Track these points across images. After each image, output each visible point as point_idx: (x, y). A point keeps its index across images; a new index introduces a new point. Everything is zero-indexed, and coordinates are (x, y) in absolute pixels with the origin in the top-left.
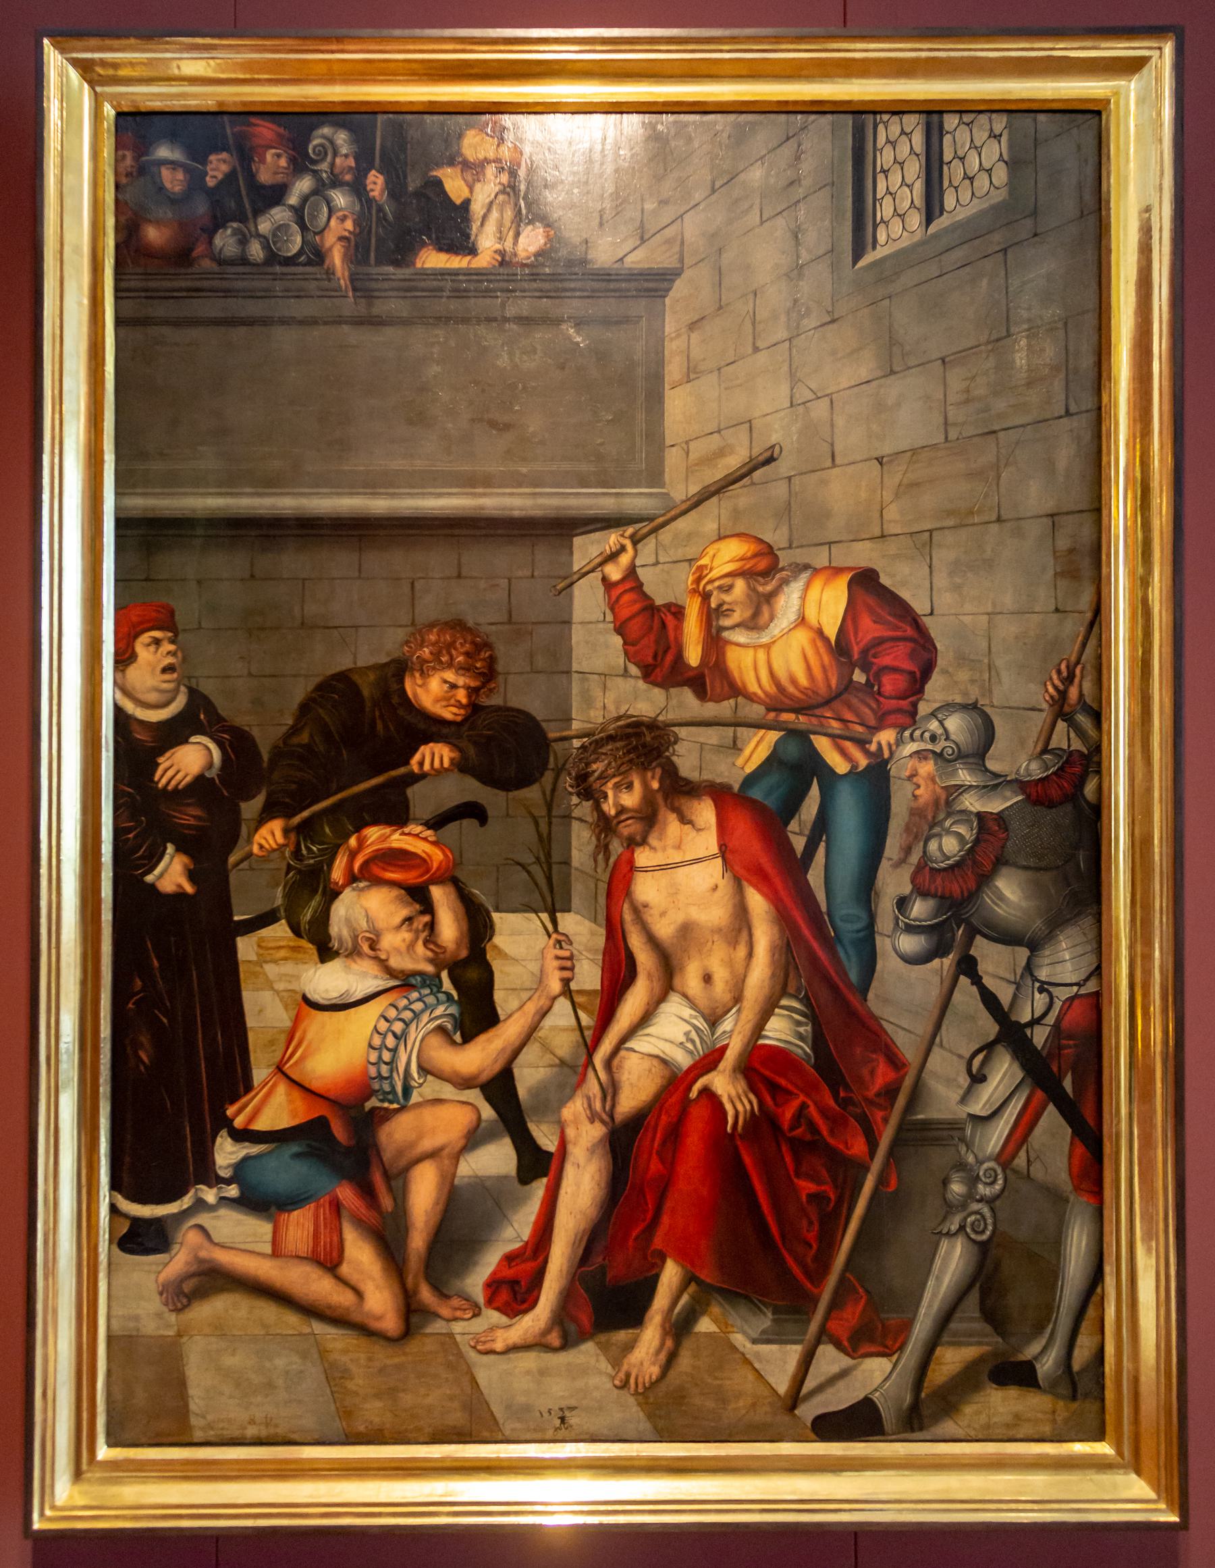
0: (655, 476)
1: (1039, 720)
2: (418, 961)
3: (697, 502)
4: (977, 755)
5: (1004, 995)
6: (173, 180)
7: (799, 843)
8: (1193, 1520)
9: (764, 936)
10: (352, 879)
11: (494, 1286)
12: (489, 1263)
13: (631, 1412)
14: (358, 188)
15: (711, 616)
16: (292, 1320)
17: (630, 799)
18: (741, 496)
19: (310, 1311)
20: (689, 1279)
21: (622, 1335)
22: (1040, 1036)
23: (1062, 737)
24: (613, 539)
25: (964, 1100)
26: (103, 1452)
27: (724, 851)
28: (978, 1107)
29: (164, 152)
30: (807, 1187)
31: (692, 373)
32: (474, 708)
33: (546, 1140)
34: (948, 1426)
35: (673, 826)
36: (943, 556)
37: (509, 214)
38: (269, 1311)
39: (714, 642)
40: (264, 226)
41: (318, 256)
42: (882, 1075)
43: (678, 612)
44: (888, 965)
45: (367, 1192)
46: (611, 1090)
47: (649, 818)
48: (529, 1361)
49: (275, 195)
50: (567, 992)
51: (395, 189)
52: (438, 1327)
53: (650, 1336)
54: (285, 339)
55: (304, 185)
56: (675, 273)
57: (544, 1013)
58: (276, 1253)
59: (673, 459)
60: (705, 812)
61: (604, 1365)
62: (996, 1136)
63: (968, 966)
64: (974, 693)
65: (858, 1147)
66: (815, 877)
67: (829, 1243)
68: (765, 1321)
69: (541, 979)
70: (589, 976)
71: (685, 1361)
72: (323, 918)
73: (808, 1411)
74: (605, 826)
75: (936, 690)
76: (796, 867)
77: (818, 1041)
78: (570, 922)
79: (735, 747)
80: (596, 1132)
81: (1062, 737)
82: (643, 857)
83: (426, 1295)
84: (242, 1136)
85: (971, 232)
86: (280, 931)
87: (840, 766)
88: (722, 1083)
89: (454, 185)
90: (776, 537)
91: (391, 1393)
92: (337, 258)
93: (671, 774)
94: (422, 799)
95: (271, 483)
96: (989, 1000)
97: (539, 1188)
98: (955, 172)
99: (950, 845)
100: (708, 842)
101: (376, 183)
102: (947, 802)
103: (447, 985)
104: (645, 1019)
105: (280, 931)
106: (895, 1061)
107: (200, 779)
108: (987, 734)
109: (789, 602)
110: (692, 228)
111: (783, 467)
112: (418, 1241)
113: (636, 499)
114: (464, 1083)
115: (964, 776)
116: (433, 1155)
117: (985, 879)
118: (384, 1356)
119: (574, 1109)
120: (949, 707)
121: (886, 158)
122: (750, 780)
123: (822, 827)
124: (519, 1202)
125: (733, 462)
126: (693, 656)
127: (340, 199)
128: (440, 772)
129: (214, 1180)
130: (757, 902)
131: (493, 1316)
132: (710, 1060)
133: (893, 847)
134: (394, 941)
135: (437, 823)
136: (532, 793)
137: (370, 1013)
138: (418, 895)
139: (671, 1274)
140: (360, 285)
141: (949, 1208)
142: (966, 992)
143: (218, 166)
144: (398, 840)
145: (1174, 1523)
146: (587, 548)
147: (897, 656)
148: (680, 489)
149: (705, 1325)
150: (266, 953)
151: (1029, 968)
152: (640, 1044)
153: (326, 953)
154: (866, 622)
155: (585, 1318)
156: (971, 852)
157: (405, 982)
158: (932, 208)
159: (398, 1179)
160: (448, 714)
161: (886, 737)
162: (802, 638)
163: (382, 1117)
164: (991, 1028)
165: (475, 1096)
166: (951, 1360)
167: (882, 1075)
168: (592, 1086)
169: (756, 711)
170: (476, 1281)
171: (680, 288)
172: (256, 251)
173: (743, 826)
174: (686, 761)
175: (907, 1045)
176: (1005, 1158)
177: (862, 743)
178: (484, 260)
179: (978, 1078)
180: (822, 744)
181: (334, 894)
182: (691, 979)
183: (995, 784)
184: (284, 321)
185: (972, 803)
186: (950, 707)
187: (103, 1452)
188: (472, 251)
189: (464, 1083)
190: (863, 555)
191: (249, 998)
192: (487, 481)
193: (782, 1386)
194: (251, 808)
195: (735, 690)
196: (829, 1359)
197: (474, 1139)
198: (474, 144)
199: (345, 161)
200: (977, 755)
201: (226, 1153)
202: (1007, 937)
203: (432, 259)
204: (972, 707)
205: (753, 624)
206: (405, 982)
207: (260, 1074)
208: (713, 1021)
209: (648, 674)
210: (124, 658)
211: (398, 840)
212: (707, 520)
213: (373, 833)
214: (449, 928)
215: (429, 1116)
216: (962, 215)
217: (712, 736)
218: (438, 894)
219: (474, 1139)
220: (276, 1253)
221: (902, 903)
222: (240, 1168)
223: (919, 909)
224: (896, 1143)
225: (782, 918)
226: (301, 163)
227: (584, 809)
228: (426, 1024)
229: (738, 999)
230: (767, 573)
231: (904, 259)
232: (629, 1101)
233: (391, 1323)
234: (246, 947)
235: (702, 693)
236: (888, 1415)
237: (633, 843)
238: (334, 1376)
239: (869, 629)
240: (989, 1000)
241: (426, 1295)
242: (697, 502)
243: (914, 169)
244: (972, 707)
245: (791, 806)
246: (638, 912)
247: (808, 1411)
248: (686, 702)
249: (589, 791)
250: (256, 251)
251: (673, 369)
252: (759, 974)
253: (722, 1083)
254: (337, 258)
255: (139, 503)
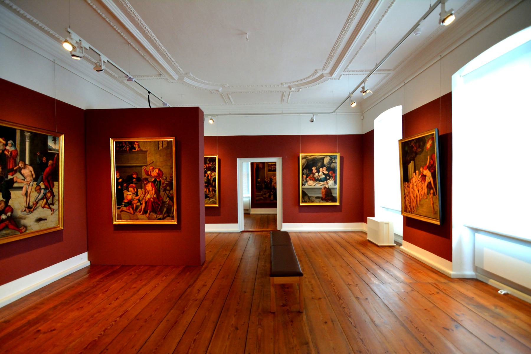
0: (147, 163)
1: (170, 177)
2: (134, 192)
3: (149, 164)
4: (166, 180)
5: (168, 194)
6: (118, 146)
7: (156, 185)
8: (183, 223)
9: (154, 191)
10: (130, 187)
11: (139, 211)
12: (138, 210)
13: (147, 219)
14: (129, 146)
15: (150, 171)
16: (127, 213)
17: (146, 182)
18: (152, 164)
19: (128, 213)
20: (150, 211)
21: (146, 214)
22: (170, 196)
23: (171, 178)
24: (144, 167)
25: (166, 200)
26: (117, 220)
27: (151, 185)
28: (167, 200)
29: (118, 144)
30: (157, 205)
31: (149, 157)
32: (136, 177)
33: (141, 203)
34: (165, 219)
35: (148, 184)
36: (164, 168)
37: (138, 147)
38: (126, 212)
39: (150, 173)
40: (124, 148)
41: (126, 150)
42: (161, 199)
43: (148, 171)
44: (161, 192)
45: (131, 206)
46: (145, 200)
47: (147, 184)
48: (141, 216)
49: (124, 146)
50: (142, 194)
51: (131, 146)
52: (135, 214)
53: (148, 214)
54: (125, 155)
55: (126, 146)
56: (147, 151)
57: (141, 195)
58: (126, 209)
59: (148, 162)
60: (150, 183)
61: (145, 216)
62: (167, 202)
63: (166, 192)
64: (166, 176)
65: (159, 203)
66: (157, 187)
67: (158, 208)
68: (154, 213)
69: (141, 193)
70: (144, 193)
71: (150, 215)
72: (128, 190)
73: (157, 218)
74: (144, 184)
75: (164, 176)
76: (156, 186)
77: (157, 197)
78: (142, 190)
79: (152, 179)
80: (144, 202)
81: (171, 178)
82: (147, 186)
83: (135, 212)
84: (124, 202)
85: (165, 148)
86: (126, 190)
87: (158, 180)
88: (152, 199)
89: (135, 146)
90: (154, 167)
91: (133, 217)
92: (128, 150)
93: (148, 181)
94: (134, 183)
95: (125, 164)
96: (167, 194)
97: (141, 205)
98: (164, 145)
99: (164, 185)
100: (151, 185)
101: (130, 146)
102: (164, 183)
103: (135, 193)
104: (147, 196)
105: (126, 190)
106: (162, 198)
107: (121, 181)
108: (166, 178)
109: (155, 170)
110: (149, 148)
111: (154, 162)
112: (134, 208)
113: (146, 164)
114: (137, 199)
115: (165, 181)
116: (135, 204)
117: (167, 187)
118: (133, 215)
119: (143, 201)
120: (164, 177)
121: (160, 144)
122: (153, 181)
123: (157, 184)
124: (140, 206)
125: (151, 162)
126: (149, 174)
127: (128, 147)
128: (135, 181)
129: (123, 205)
130: (153, 189)
131: (139, 213)
132: (151, 198)
133: (161, 185)
134: (132, 191)
135: (135, 184)
136: (140, 182)
137: (131, 195)
138: (134, 188)
139: (149, 211)
140: (129, 152)
141: (165, 206)
142: (166, 194)
143: (121, 145)
144: (132, 185)
145: (174, 225)
146: (143, 167)
147: (161, 174)
148: (148, 163)
149: (151, 213)
150: (125, 192)
151: (169, 192)
152: (147, 197)
153: (129, 192)
154: (159, 172)
155: (144, 213)
156: (166, 185)
157: (133, 193)
158: (163, 147)
159: (133, 205)
160: (135, 177)
161: (161, 179)
162: (155, 173)
163: (132, 201)
164: (167, 196)
165: (137, 200)
166: (165, 215)
167: (161, 199)
168: (144, 200)
169: (153, 177)
170: (138, 211)
171: (148, 152)
172: (123, 150)
173: (152, 184)
174: (149, 180)
175: (162, 197)
176: (168, 203)
177: (159, 179)
178: (136, 150)
179: (166, 199)
180: (157, 179)
181: (129, 188)
182: (150, 193)
183: (167, 181)
184: (125, 154)
185: (166, 182)
186: (164, 177)
187: (117, 220)
188: (136, 150)
189: (137, 199)
190: (159, 168)
191: (124, 194)
192: (137, 164)
193: (155, 217)
194: (124, 183)
195: (152, 176)
196: (158, 215)
197: (137, 203)
198: (136, 143)
199: (128, 144)
200: (166, 180)
201: (123, 203)
202: (168, 190)
203: (133, 150)
204: (165, 177)
205: (153, 172)
206: (133, 193)
207: (125, 199)
208: (151, 196)
209: (147, 175)
210: (116, 174)
211: (132, 185)
212: (150, 165)
213: (131, 185)
214: (136, 190)
215: (135, 201)
216: (165, 147)
217: (151, 179)
218: (135, 188)
219: (137, 203)
220: (126, 209)
221: (162, 189)
222: (124, 204)
223: (163, 189)
224: (162, 203)
225: (155, 190)
226: (126, 145)
227: (143, 183)
228: (134, 196)
229: (152, 194)
230: (154, 169)
231: (161, 150)
232: (146, 200)
233: (133, 213)
234: (124, 191)
235: (150, 176)
236: (162, 219)
237: (146, 185)
238: (130, 216)
239: (159, 172)
240: (167, 194)
241: (135, 212)
242: (149, 164)
243: (161, 144)
244: (165, 177)
245: (155, 183)
246: (147, 189)
247: (157, 218)
248: (149, 177)
249: (144, 182)
250: (123, 150)
251: (148, 157)
252: (154, 193)
253: (152, 199)
254: (128, 150)
255: (117, 165)
